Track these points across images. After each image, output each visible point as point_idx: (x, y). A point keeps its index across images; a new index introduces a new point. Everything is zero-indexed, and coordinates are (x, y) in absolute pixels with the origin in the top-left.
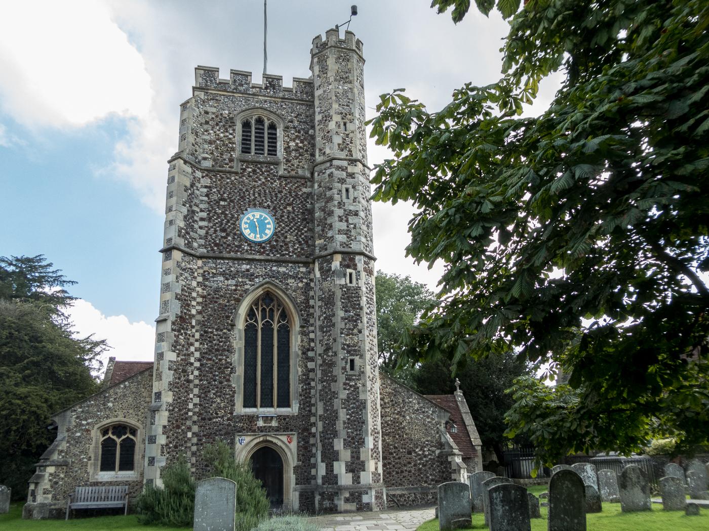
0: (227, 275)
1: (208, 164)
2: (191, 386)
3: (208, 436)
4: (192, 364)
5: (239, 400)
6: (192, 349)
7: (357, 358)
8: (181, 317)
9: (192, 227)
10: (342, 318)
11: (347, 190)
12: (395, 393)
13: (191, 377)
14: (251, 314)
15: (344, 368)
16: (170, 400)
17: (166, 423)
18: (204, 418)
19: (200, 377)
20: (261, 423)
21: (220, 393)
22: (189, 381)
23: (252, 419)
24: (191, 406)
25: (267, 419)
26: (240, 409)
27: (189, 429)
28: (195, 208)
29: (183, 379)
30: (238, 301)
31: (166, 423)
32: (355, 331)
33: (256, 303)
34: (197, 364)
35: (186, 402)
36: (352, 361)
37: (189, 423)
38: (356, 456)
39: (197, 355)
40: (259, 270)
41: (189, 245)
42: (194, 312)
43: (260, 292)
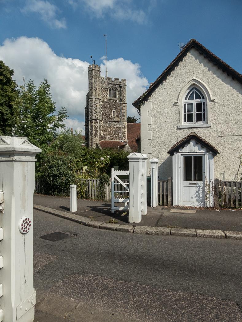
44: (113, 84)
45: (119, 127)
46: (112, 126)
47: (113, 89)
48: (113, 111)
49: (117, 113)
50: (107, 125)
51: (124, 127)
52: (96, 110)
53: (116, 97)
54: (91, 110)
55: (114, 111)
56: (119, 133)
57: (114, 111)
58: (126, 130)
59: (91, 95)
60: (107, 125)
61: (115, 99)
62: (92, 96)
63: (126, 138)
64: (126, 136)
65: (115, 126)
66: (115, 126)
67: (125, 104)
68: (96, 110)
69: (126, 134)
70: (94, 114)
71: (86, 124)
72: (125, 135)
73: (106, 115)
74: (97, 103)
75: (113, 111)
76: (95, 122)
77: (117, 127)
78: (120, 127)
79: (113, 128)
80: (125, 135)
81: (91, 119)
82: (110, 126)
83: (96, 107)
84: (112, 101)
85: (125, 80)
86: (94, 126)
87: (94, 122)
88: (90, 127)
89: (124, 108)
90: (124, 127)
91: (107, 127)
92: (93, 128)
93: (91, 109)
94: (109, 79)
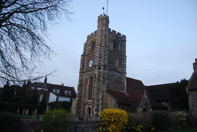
0: (87, 75)
1: (87, 55)
5: (87, 99)
8: (80, 84)
9: (84, 68)
14: (90, 82)
16: (78, 99)
23: (88, 102)
25: (90, 102)
28: (84, 64)
30: (88, 79)
35: (81, 99)
38: (93, 110)
41: (83, 71)
42: (83, 83)
43: (91, 77)
44: (117, 37)
47: (116, 41)
50: (111, 74)
52: (105, 57)
53: (118, 49)
57: (117, 62)
58: (126, 81)
59: (100, 41)
60: (111, 74)
61: (118, 50)
64: (126, 87)
65: (117, 76)
66: (117, 76)
68: (105, 57)
69: (126, 85)
70: (104, 60)
71: (81, 71)
72: (125, 86)
73: (111, 63)
74: (106, 50)
76: (104, 69)
79: (116, 77)
80: (125, 86)
85: (125, 36)
87: (102, 68)
89: (124, 60)
91: (111, 76)
92: (102, 74)
93: (100, 54)
94: (114, 32)
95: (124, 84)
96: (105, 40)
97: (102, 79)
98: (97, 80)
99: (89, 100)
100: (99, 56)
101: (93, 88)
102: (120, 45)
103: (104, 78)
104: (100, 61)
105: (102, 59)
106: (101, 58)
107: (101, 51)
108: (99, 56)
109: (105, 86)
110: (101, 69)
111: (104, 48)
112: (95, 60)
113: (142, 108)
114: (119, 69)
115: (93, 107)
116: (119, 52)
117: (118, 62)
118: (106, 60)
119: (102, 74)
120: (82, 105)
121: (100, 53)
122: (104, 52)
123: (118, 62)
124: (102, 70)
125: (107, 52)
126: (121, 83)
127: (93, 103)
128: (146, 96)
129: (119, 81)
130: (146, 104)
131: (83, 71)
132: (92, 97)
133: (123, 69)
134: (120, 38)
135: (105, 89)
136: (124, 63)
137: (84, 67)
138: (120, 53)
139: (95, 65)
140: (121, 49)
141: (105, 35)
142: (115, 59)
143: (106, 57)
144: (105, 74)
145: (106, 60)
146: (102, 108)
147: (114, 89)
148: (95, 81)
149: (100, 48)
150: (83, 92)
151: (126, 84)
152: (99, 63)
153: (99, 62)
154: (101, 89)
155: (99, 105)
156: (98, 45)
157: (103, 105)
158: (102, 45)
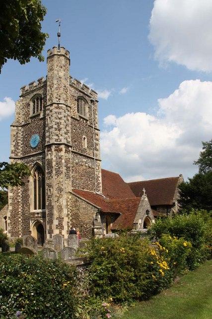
2: (20, 203)
3: (24, 220)
4: (19, 196)
6: (20, 191)
7: (51, 188)
10: (47, 173)
11: (50, 118)
12: (77, 201)
13: (20, 200)
15: (47, 193)
17: (10, 216)
18: (23, 214)
19: (22, 200)
20: (36, 215)
21: (27, 206)
22: (19, 202)
23: (34, 213)
24: (20, 210)
25: (38, 213)
26: (32, 210)
27: (20, 218)
29: (16, 201)
31: (10, 216)
32: (51, 177)
33: (35, 171)
34: (21, 196)
36: (50, 190)
37: (19, 216)
38: (51, 228)
39: (21, 193)
40: (35, 158)
45: (92, 168)
46: (83, 164)
48: (83, 137)
49: (88, 142)
50: (77, 161)
51: (97, 168)
52: (68, 128)
53: (85, 115)
54: (58, 126)
55: (84, 138)
56: (92, 178)
58: (100, 175)
62: (59, 99)
63: (101, 188)
64: (101, 185)
65: (87, 165)
66: (87, 165)
67: (98, 130)
68: (68, 128)
69: (101, 182)
70: (65, 133)
73: (75, 141)
75: (83, 137)
76: (66, 151)
77: (90, 167)
78: (93, 167)
79: (84, 167)
80: (99, 184)
81: (60, 143)
82: (81, 163)
83: (67, 122)
84: (82, 119)
86: (64, 158)
87: (64, 149)
88: (54, 159)
89: (97, 137)
90: (97, 168)
91: (77, 164)
92: (63, 161)
93: (58, 123)
95: (98, 180)
96: (65, 96)
97: (64, 169)
98: (54, 172)
99: (35, 209)
100: (55, 126)
101: (46, 187)
102: (89, 108)
103: (68, 168)
104: (57, 135)
105: (63, 131)
106: (59, 130)
107: (60, 116)
108: (55, 126)
109: (71, 184)
110: (61, 150)
111: (65, 112)
112: (47, 134)
113: (142, 219)
114: (89, 153)
115: (51, 222)
116: (87, 120)
117: (86, 140)
118: (69, 134)
119: (63, 161)
120: (20, 220)
121: (58, 121)
122: (65, 119)
123: (86, 140)
124: (63, 153)
125: (69, 118)
126: (93, 178)
127: (51, 215)
128: (146, 199)
129: (89, 174)
130: (147, 212)
131: (17, 155)
132: (47, 204)
133: (95, 152)
134: (88, 96)
135: (70, 189)
136: (97, 142)
137: (19, 147)
138: (88, 122)
139: (46, 144)
140: (90, 115)
141: (65, 86)
142: (82, 134)
143: (69, 128)
144: (69, 161)
145: (69, 134)
146: (68, 222)
147: (83, 189)
148: (50, 173)
149: (57, 110)
150: (20, 194)
151: (100, 179)
152: (56, 140)
153: (57, 137)
154: (63, 187)
155: (63, 218)
156: (51, 105)
157: (69, 218)
158: (60, 105)
